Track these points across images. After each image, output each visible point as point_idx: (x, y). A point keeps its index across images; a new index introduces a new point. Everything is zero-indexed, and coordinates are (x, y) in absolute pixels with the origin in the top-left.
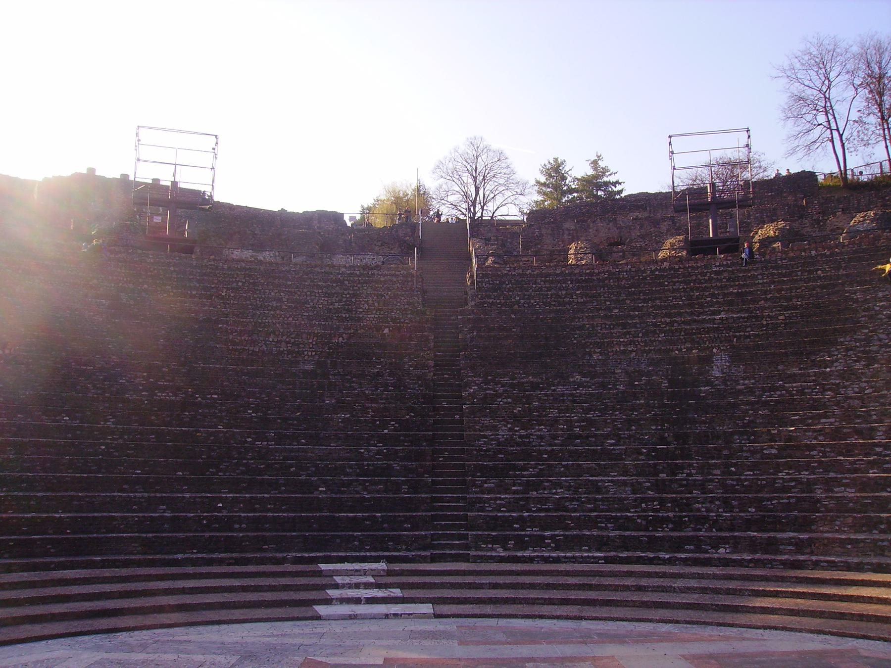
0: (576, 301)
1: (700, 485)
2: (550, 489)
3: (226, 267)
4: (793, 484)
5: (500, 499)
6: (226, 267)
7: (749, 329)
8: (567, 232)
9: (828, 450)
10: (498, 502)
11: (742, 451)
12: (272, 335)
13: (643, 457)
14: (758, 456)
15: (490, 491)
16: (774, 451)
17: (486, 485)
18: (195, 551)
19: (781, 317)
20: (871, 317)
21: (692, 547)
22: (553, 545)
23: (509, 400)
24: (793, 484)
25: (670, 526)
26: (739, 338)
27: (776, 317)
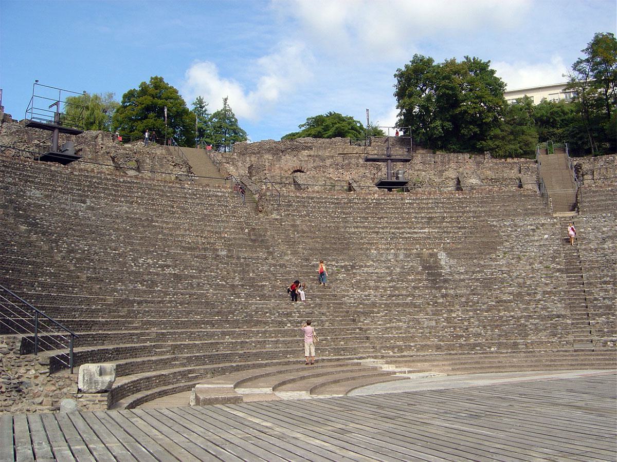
0: (341, 216)
1: (468, 319)
2: (396, 323)
3: (122, 180)
4: (511, 318)
5: (379, 328)
6: (122, 180)
7: (446, 239)
8: (267, 161)
9: (519, 302)
10: (378, 330)
11: (478, 303)
12: (188, 232)
13: (430, 306)
14: (486, 305)
15: (368, 324)
16: (493, 303)
17: (365, 321)
18: (260, 360)
19: (460, 233)
20: (508, 236)
21: (479, 348)
22: (415, 350)
23: (345, 275)
24: (511, 318)
25: (464, 339)
26: (444, 244)
27: (458, 232)
